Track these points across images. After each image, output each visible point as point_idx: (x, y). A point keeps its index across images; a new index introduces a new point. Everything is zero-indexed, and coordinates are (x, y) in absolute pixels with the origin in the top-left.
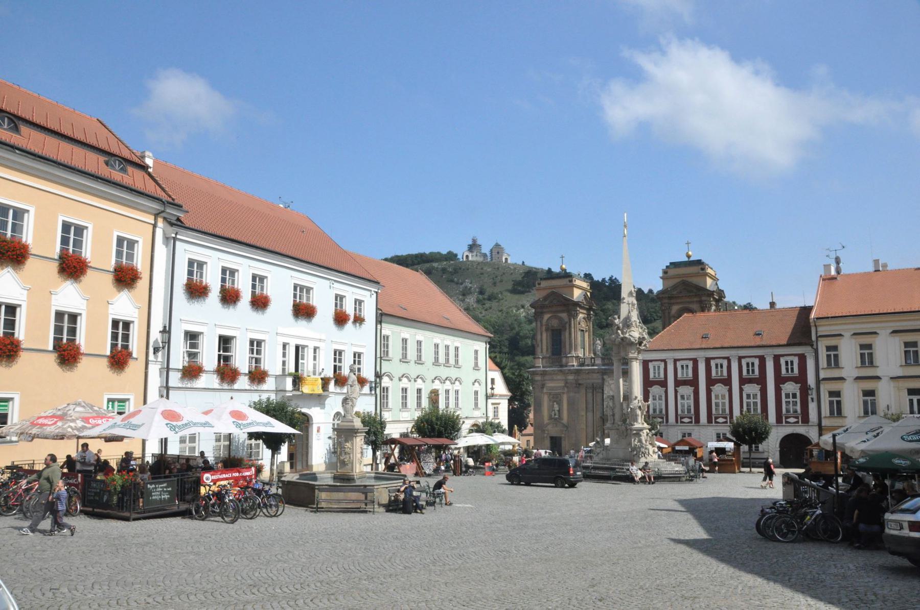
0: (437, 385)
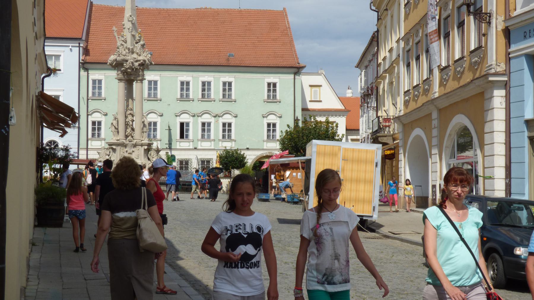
0: (185, 118)
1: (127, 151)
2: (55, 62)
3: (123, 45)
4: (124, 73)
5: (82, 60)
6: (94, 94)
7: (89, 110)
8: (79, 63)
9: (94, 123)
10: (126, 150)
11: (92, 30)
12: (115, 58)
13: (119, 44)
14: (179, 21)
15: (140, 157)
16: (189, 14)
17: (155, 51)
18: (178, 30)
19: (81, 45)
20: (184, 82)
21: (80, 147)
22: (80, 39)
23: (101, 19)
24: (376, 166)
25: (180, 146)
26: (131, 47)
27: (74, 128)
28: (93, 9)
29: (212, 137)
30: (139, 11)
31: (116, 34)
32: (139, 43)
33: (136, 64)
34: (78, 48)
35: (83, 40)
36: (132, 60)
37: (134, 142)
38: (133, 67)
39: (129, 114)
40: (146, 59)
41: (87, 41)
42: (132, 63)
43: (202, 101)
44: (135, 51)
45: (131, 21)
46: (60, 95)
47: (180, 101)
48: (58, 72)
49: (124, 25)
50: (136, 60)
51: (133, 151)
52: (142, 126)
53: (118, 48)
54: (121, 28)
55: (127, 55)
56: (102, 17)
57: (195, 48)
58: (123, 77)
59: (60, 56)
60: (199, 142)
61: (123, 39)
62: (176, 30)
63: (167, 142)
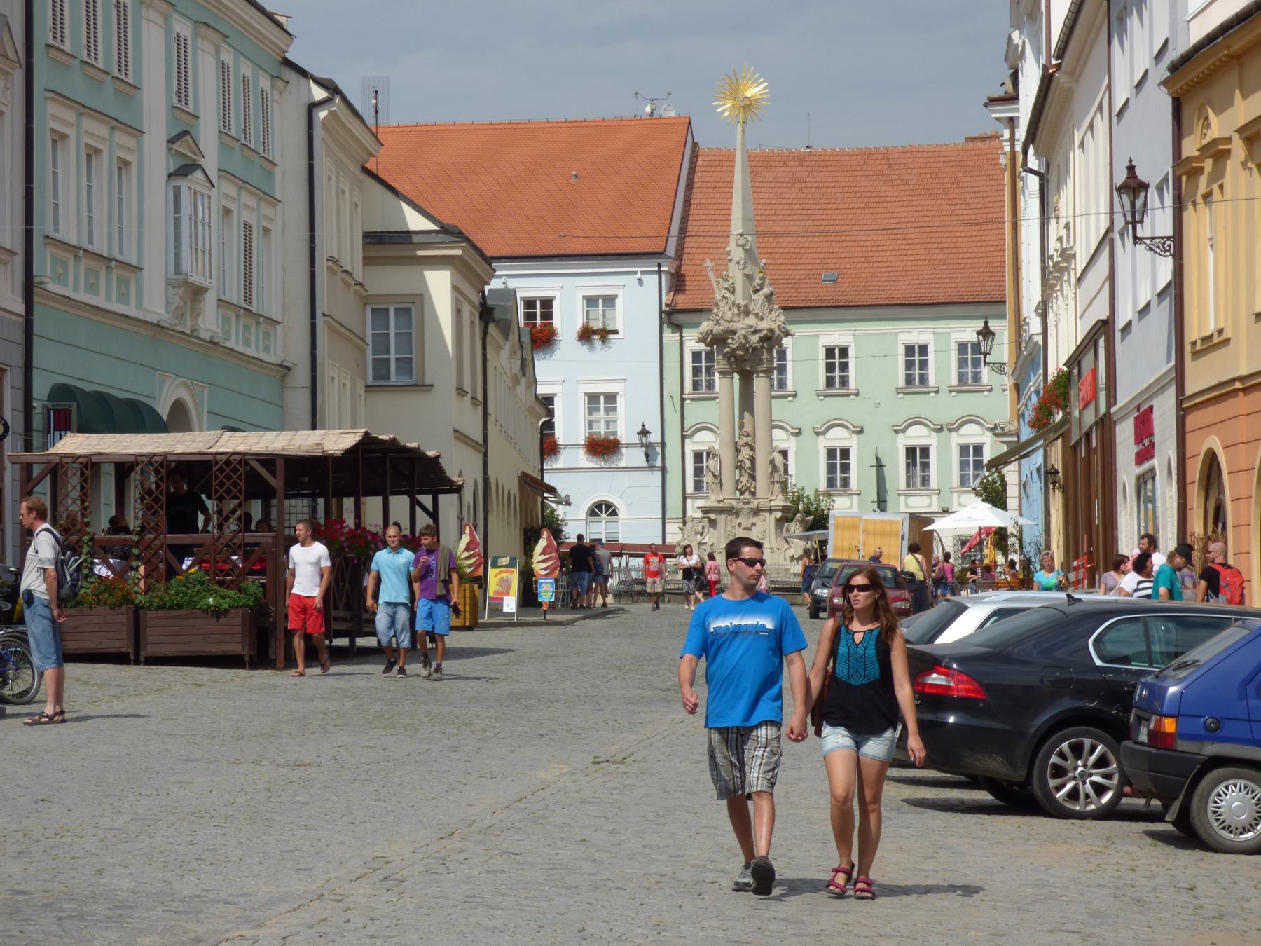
0: (918, 435)
1: (740, 524)
2: (604, 311)
3: (726, 298)
4: (729, 358)
5: (667, 305)
6: (696, 385)
7: (687, 426)
8: (661, 312)
9: (698, 457)
10: (738, 521)
11: (694, 223)
12: (710, 328)
13: (718, 296)
14: (914, 182)
15: (767, 535)
16: (942, 159)
17: (846, 271)
18: (909, 209)
19: (662, 269)
20: (913, 347)
21: (667, 516)
22: (661, 254)
23: (716, 190)
24: (903, 538)
25: (907, 506)
26: (743, 303)
27: (652, 471)
28: (700, 163)
29: (934, 483)
30: (815, 158)
31: (711, 275)
32: (761, 292)
33: (754, 339)
34: (656, 277)
35: (670, 258)
36: (744, 332)
37: (755, 503)
38: (747, 345)
39: (743, 446)
40: (774, 326)
41: (679, 256)
42: (745, 337)
43: (958, 392)
44: (751, 309)
45: (743, 246)
46: (618, 393)
47: (904, 393)
48: (611, 336)
49: (728, 253)
50: (753, 329)
51: (753, 524)
52: (770, 470)
53: (717, 305)
54: (723, 260)
55: (736, 319)
56: (720, 185)
57: (946, 256)
58: (727, 367)
59: (616, 296)
60: (955, 495)
61: (726, 286)
62: (903, 209)
63: (875, 498)
